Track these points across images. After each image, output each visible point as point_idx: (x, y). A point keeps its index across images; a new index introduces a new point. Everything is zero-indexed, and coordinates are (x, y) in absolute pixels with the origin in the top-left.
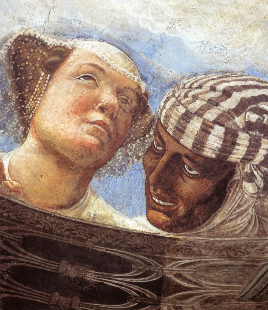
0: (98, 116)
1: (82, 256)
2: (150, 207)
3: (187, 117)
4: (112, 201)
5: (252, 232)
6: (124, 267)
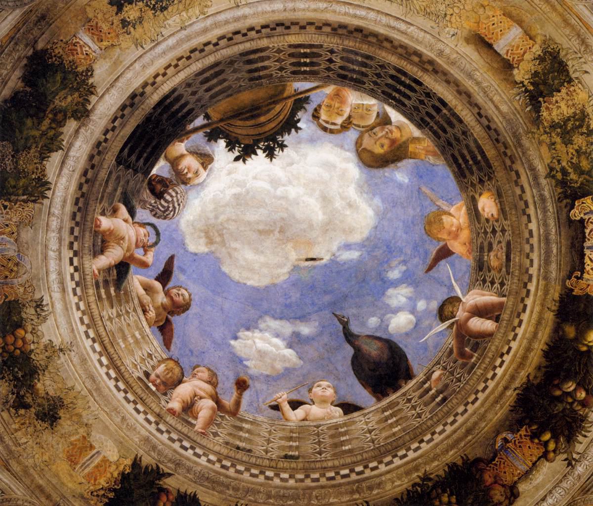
0: (186, 171)
1: (151, 154)
2: (157, 176)
3: (177, 193)
4: (162, 167)
5: (141, 198)
6: (145, 164)
